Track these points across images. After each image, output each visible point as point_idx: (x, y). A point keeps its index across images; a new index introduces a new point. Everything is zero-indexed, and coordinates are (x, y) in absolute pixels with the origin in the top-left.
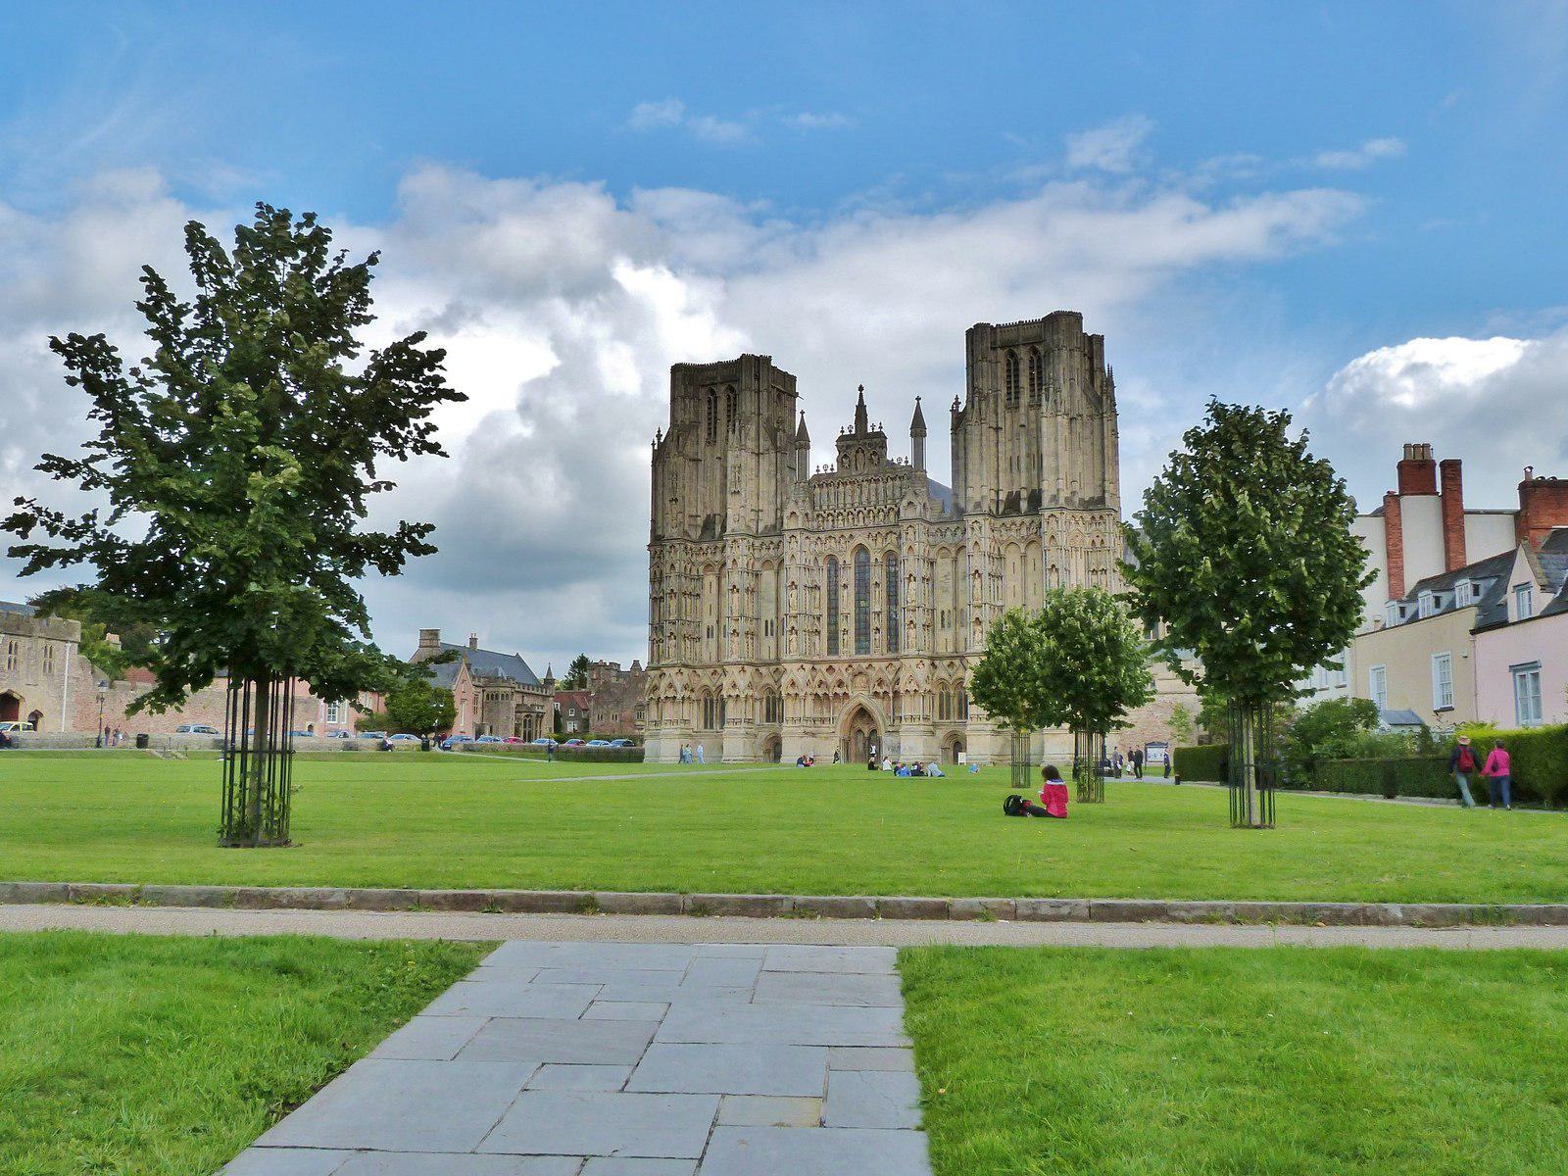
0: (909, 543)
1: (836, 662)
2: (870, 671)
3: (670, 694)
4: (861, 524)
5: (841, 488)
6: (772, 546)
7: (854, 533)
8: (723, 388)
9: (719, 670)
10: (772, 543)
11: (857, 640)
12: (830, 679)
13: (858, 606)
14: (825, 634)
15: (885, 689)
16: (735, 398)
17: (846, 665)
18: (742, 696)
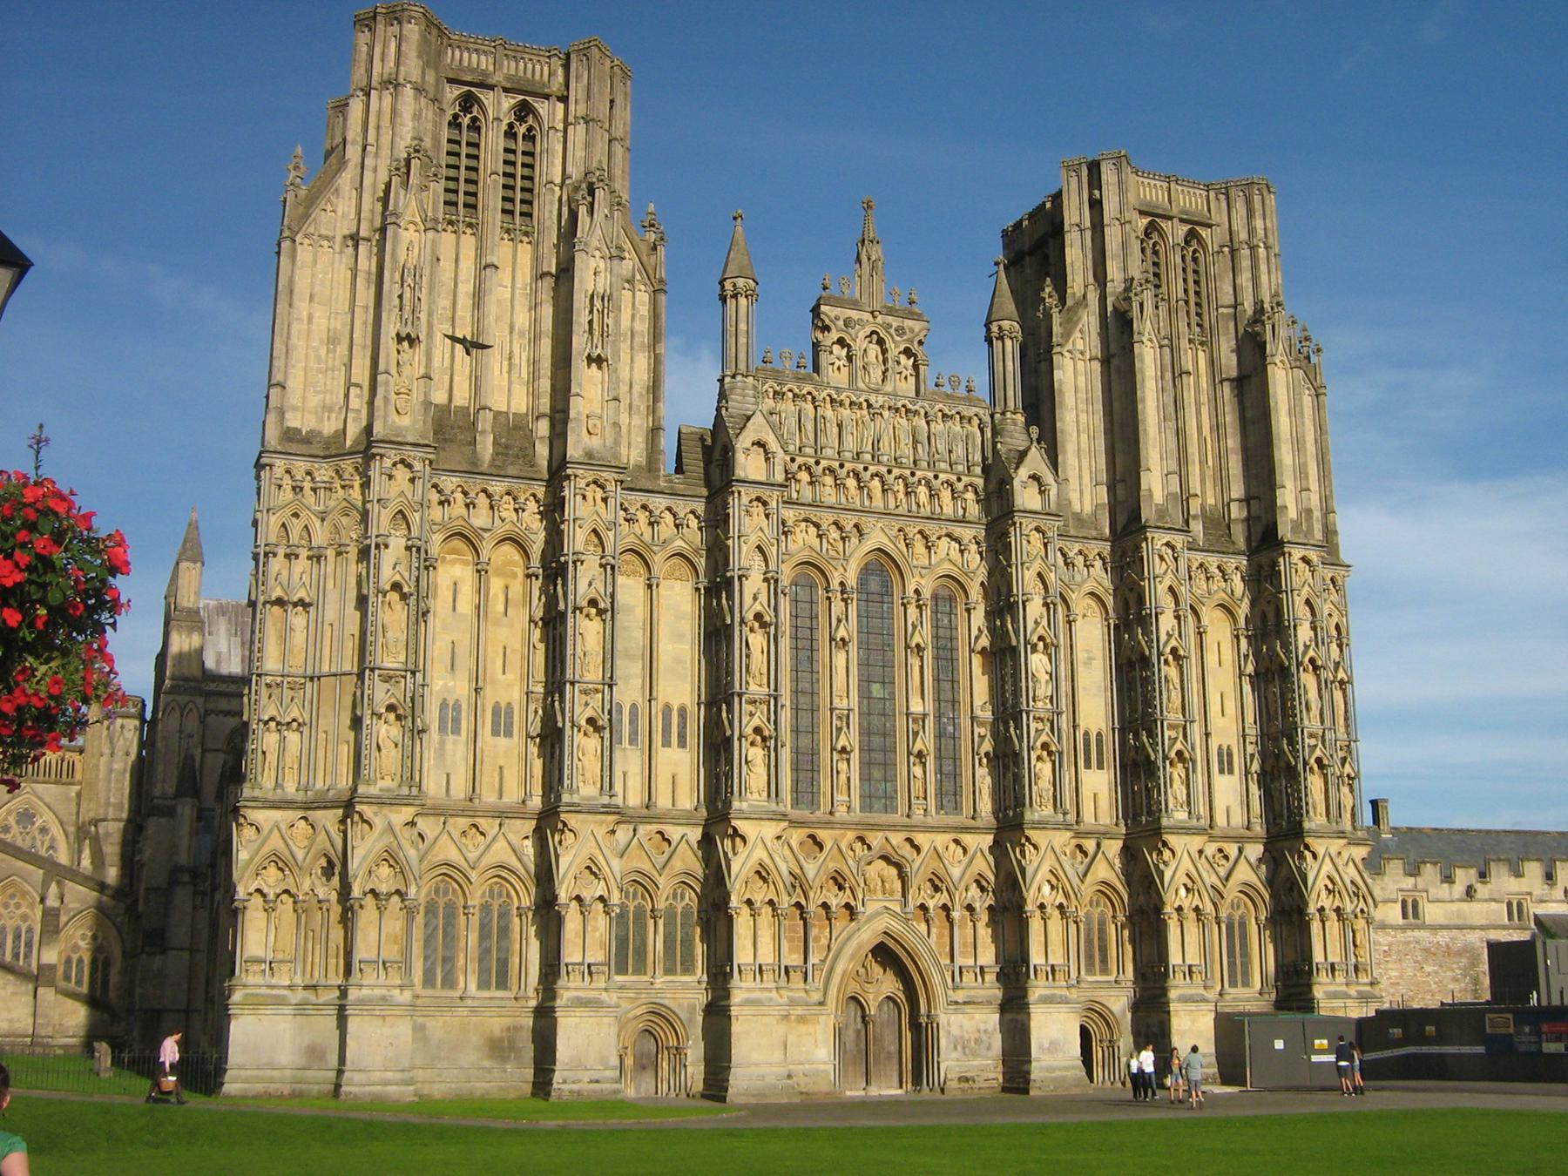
0: (1037, 566)
1: (828, 825)
2: (907, 851)
3: (385, 879)
4: (878, 503)
5: (829, 413)
6: (642, 517)
7: (867, 522)
8: (508, 102)
9: (483, 823)
10: (644, 507)
11: (865, 778)
12: (811, 869)
13: (865, 695)
14: (786, 755)
15: (943, 898)
16: (530, 137)
17: (851, 835)
18: (615, 898)
